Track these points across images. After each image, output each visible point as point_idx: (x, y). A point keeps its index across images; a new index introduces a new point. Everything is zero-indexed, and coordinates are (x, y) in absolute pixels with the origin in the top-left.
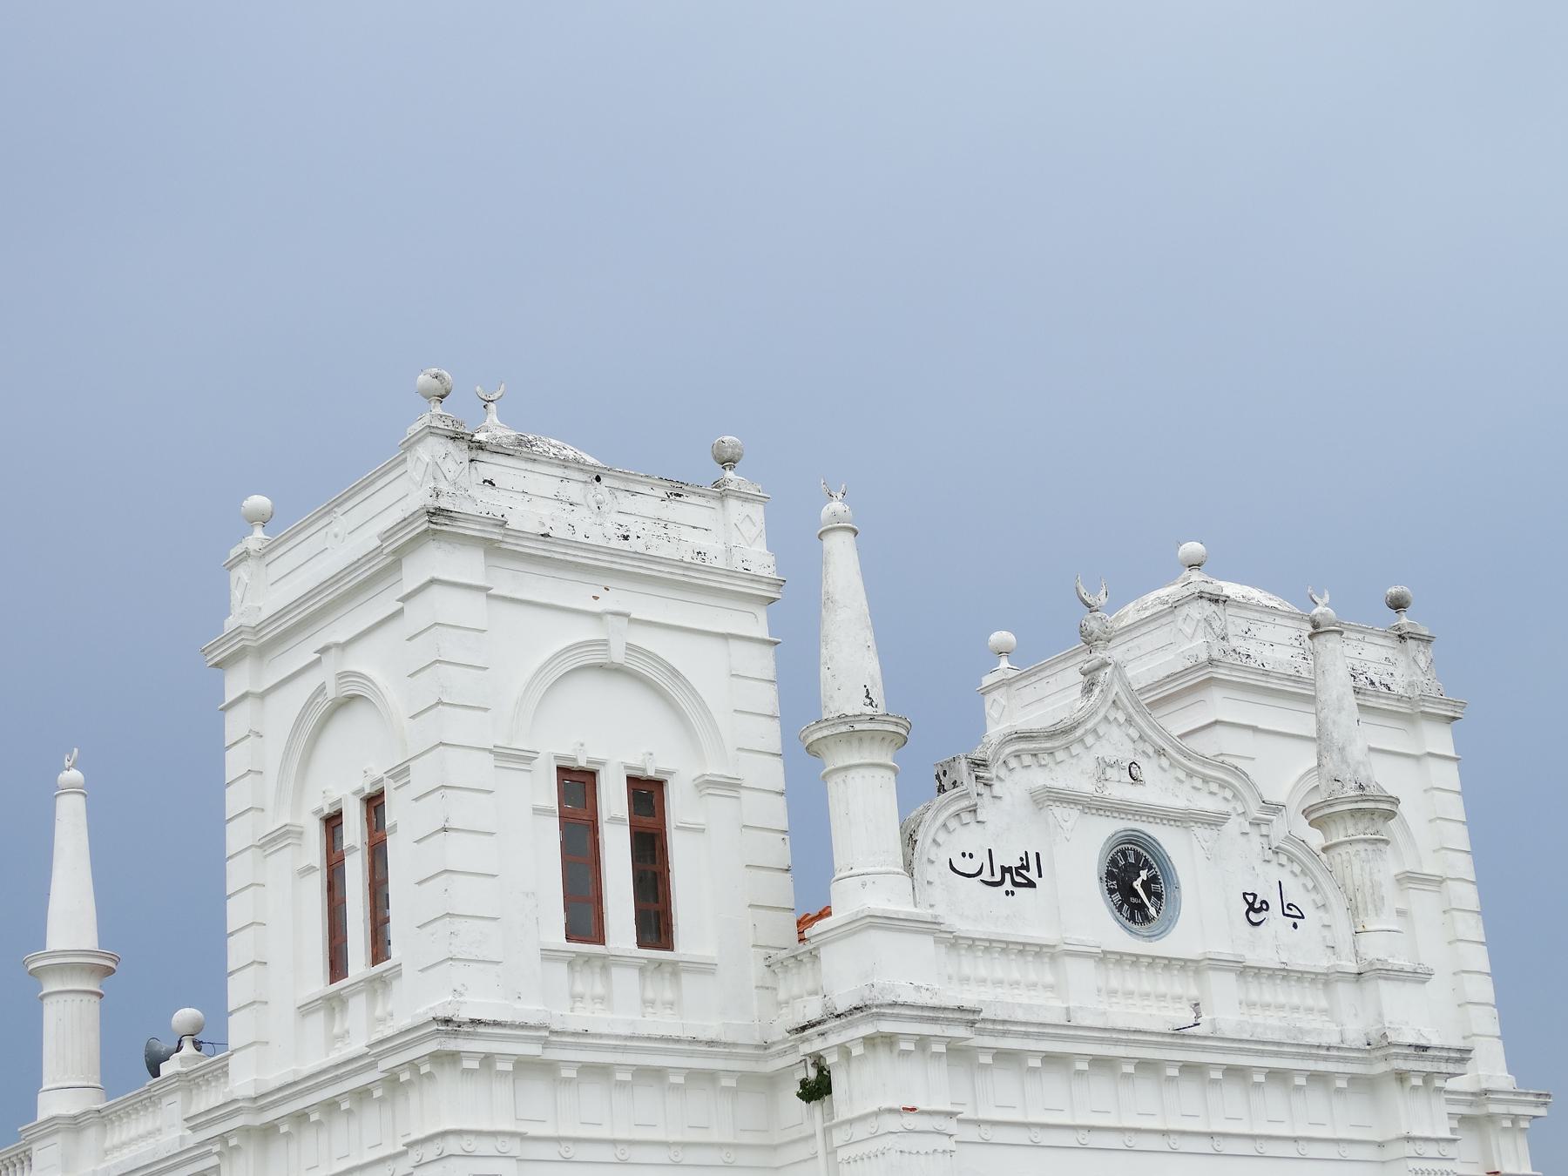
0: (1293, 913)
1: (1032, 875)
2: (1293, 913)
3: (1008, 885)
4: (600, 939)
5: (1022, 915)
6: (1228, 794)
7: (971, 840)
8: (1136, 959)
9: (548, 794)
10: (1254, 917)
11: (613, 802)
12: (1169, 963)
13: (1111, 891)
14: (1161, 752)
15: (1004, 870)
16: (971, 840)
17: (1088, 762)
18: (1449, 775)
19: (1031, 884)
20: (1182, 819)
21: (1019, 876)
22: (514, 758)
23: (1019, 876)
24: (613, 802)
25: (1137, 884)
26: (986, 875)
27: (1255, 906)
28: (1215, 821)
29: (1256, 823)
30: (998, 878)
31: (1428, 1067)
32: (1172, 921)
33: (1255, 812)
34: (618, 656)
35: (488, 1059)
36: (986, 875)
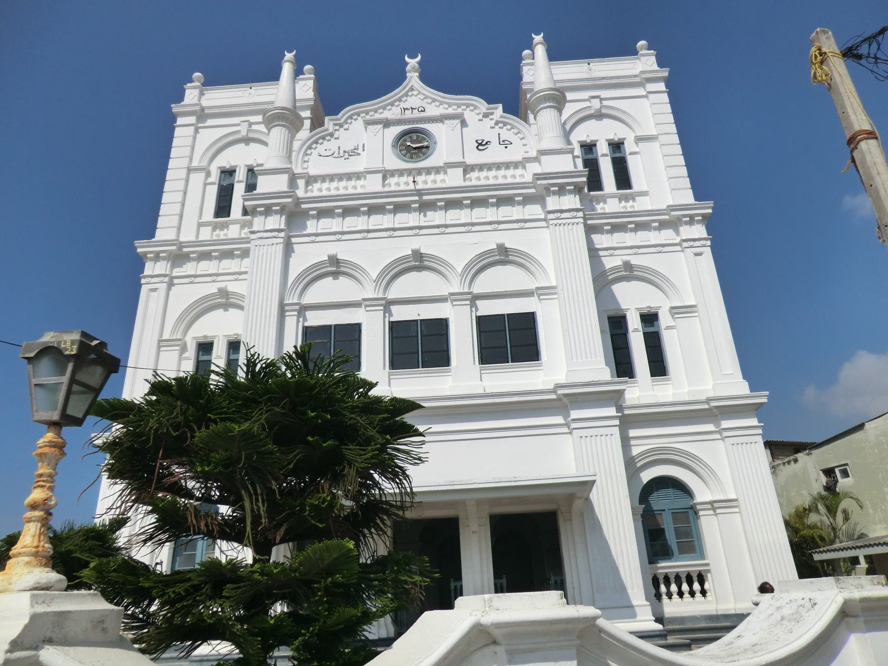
0: (505, 144)
2: (505, 144)
3: (346, 156)
8: (409, 172)
9: (215, 177)
10: (480, 147)
12: (428, 171)
13: (401, 151)
15: (345, 152)
18: (665, 98)
20: (441, 119)
21: (353, 153)
23: (353, 153)
26: (336, 155)
27: (481, 145)
30: (342, 154)
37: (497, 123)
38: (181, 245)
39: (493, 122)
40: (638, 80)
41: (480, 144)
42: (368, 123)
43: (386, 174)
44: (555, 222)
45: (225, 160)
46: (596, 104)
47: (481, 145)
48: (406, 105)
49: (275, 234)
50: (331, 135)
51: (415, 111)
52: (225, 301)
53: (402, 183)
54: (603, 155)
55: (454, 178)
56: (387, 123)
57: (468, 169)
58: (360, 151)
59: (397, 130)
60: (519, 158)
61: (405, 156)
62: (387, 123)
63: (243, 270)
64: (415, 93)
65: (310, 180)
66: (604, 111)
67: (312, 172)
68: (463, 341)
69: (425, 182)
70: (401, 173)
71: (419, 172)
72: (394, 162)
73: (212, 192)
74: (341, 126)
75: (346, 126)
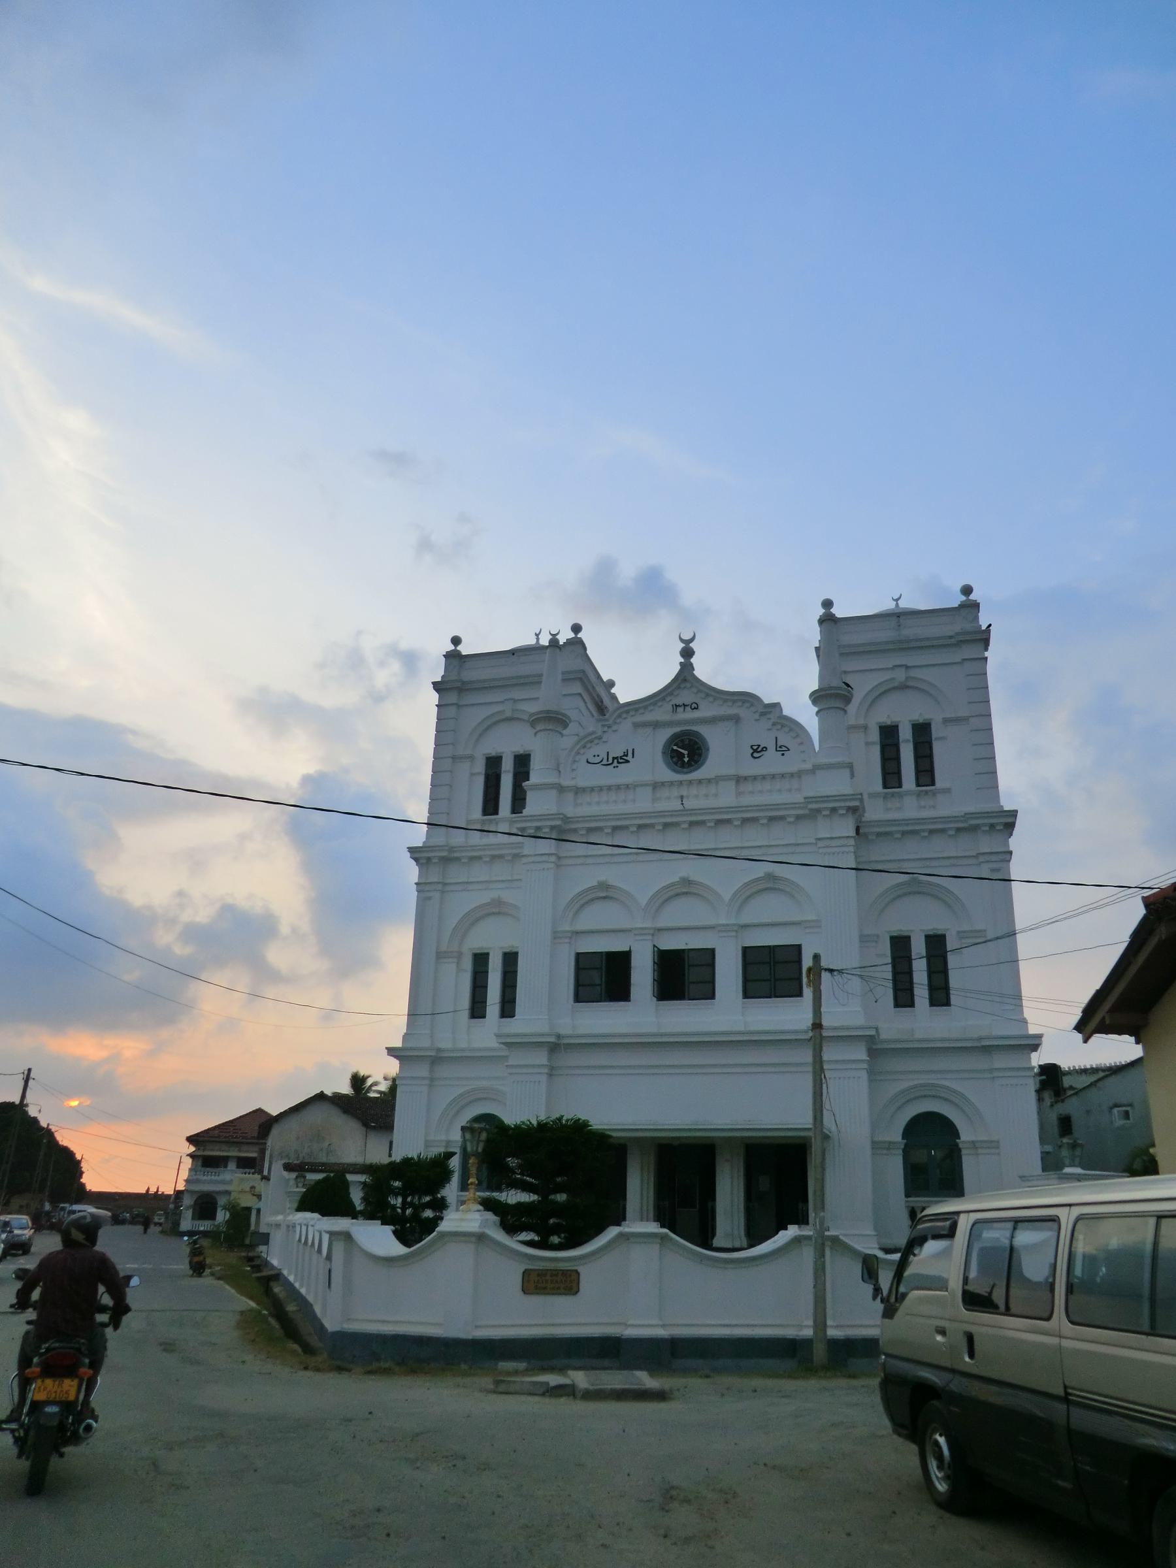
0: (782, 749)
1: (629, 758)
2: (782, 749)
4: (496, 812)
5: (623, 775)
6: (747, 705)
7: (600, 750)
8: (681, 782)
9: (480, 767)
10: (756, 755)
11: (507, 766)
12: (700, 782)
14: (707, 695)
16: (600, 750)
17: (668, 707)
19: (627, 761)
21: (622, 759)
22: (471, 758)
23: (622, 759)
24: (507, 766)
25: (686, 752)
28: (736, 719)
29: (763, 714)
31: (831, 805)
32: (703, 764)
33: (761, 710)
34: (508, 714)
35: (429, 859)
36: (605, 762)
37: (774, 724)
38: (451, 849)
39: (770, 723)
40: (953, 641)
41: (755, 751)
42: (637, 725)
43: (656, 786)
44: (825, 850)
45: (490, 747)
46: (900, 675)
47: (757, 751)
48: (679, 701)
49: (544, 858)
50: (600, 738)
51: (688, 709)
52: (497, 909)
53: (669, 803)
54: (908, 741)
55: (726, 797)
56: (656, 725)
57: (739, 780)
58: (629, 758)
59: (665, 734)
60: (794, 769)
61: (676, 764)
62: (656, 725)
63: (515, 877)
64: (688, 685)
65: (578, 791)
66: (911, 683)
67: (581, 783)
68: (728, 973)
69: (697, 799)
70: (672, 783)
71: (690, 782)
72: (666, 774)
73: (480, 783)
74: (609, 727)
75: (615, 728)
